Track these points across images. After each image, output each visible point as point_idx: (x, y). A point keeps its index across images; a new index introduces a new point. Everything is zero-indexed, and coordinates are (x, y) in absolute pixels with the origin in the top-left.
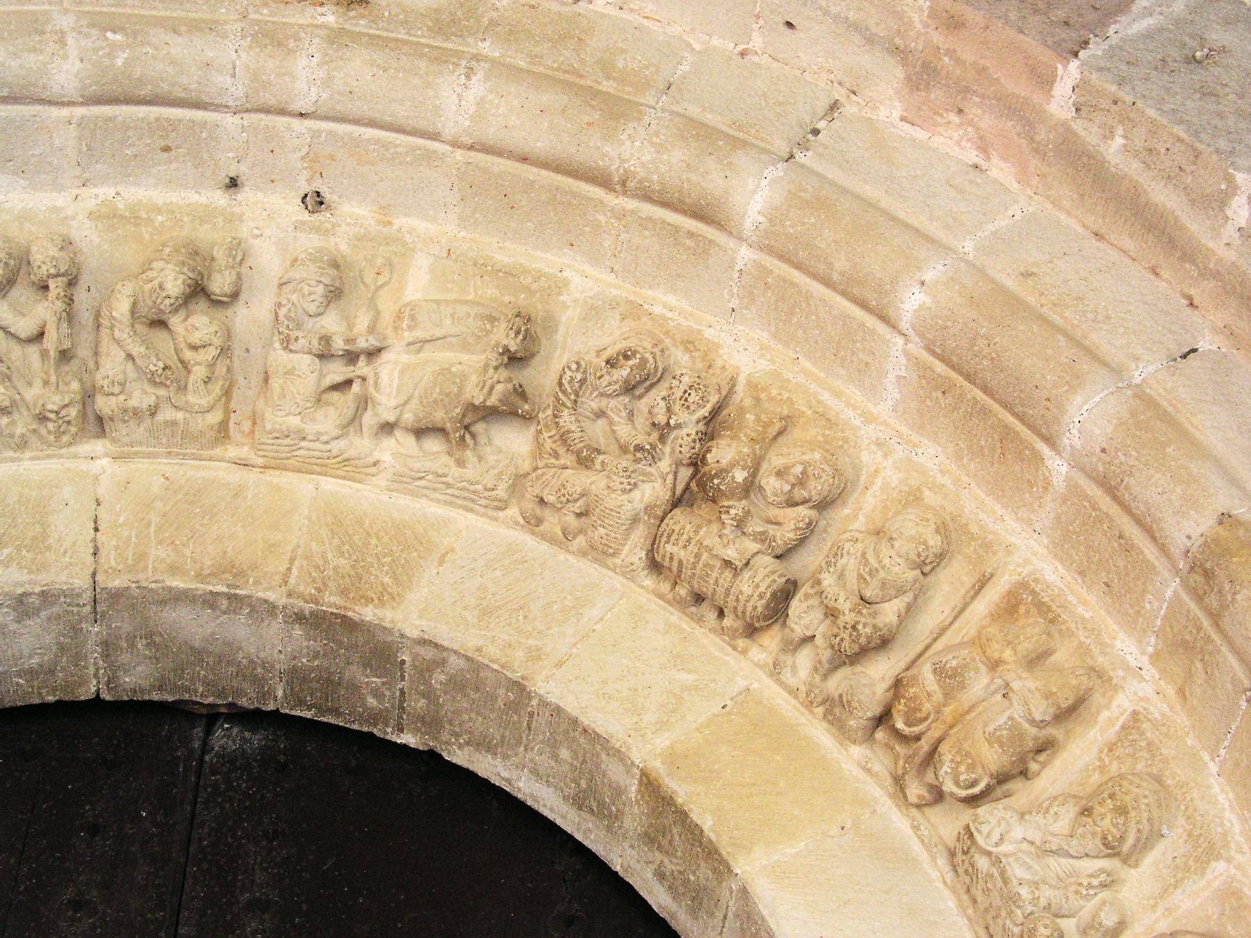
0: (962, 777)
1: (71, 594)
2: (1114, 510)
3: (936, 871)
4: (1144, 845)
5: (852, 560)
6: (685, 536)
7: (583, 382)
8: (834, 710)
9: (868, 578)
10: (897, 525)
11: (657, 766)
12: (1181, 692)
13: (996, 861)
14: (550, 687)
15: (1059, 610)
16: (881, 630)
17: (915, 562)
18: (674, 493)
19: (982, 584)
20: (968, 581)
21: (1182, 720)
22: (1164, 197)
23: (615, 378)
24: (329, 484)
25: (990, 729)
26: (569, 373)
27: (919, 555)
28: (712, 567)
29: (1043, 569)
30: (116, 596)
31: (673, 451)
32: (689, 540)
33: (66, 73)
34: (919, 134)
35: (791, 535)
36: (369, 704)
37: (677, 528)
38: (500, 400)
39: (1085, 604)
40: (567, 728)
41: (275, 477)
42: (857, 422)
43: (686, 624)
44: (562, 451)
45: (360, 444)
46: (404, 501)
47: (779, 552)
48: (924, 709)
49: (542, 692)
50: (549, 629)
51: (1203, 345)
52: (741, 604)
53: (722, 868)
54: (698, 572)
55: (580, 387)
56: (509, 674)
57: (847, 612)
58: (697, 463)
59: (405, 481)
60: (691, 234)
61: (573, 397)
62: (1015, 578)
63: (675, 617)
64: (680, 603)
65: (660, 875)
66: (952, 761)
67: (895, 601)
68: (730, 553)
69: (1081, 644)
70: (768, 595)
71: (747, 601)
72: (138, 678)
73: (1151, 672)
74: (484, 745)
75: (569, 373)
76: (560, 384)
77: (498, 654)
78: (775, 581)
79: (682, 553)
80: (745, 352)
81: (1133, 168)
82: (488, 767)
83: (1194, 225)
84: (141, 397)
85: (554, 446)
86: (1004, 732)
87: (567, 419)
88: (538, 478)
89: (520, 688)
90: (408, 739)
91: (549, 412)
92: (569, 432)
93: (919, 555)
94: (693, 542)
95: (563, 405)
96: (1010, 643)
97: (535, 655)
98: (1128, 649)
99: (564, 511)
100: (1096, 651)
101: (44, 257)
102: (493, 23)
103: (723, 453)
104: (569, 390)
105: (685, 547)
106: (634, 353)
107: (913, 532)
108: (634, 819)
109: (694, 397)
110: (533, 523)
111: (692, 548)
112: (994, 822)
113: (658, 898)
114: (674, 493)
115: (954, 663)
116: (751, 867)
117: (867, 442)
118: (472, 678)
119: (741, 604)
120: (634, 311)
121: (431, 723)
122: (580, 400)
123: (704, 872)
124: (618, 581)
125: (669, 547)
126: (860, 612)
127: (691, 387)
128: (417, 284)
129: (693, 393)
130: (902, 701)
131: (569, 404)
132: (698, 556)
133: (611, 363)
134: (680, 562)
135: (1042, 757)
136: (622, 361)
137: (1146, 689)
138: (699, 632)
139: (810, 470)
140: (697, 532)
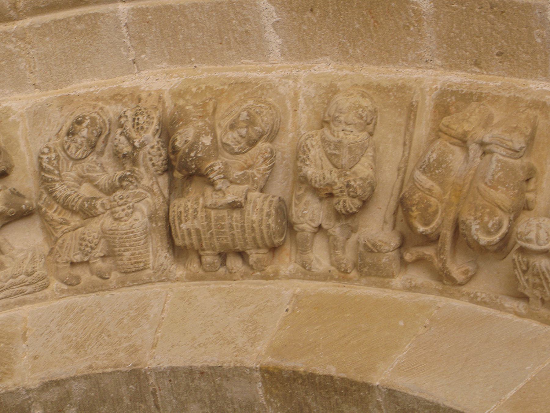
0: (490, 225)
5: (317, 150)
6: (191, 211)
7: (58, 158)
9: (337, 152)
10: (333, 109)
14: (159, 359)
15: (479, 91)
16: (367, 179)
17: (361, 124)
18: (163, 196)
20: (402, 120)
23: (79, 140)
25: (489, 177)
26: (45, 157)
27: (361, 117)
28: (222, 218)
29: (449, 79)
31: (147, 169)
32: (195, 210)
35: (264, 167)
37: (182, 209)
38: (6, 205)
42: (262, 75)
44: (68, 216)
47: (261, 183)
48: (432, 203)
49: (154, 366)
50: (131, 333)
52: (257, 231)
54: (214, 230)
55: (58, 162)
56: (122, 369)
57: (336, 180)
60: (79, 19)
61: (56, 172)
62: (434, 95)
66: (475, 219)
67: (363, 159)
68: (230, 198)
69: (509, 99)
70: (273, 212)
71: (260, 225)
75: (45, 157)
76: (42, 168)
77: (106, 363)
78: (271, 201)
79: (196, 223)
85: (61, 216)
86: (500, 174)
87: (60, 190)
88: (61, 247)
89: (137, 375)
91: (45, 196)
92: (67, 196)
93: (361, 117)
94: (199, 210)
95: (53, 181)
96: (463, 120)
99: (91, 262)
100: (522, 95)
104: (52, 168)
105: (195, 217)
106: (84, 117)
107: (348, 104)
109: (142, 119)
111: (201, 214)
112: (534, 228)
114: (164, 198)
115: (434, 156)
117: (277, 80)
119: (257, 231)
122: (62, 174)
125: (184, 226)
126: (345, 175)
127: (136, 115)
129: (141, 117)
130: (414, 208)
131: (56, 178)
132: (208, 217)
133: (71, 133)
134: (197, 231)
135: (532, 186)
136: (78, 127)
139: (252, 111)
140: (197, 203)
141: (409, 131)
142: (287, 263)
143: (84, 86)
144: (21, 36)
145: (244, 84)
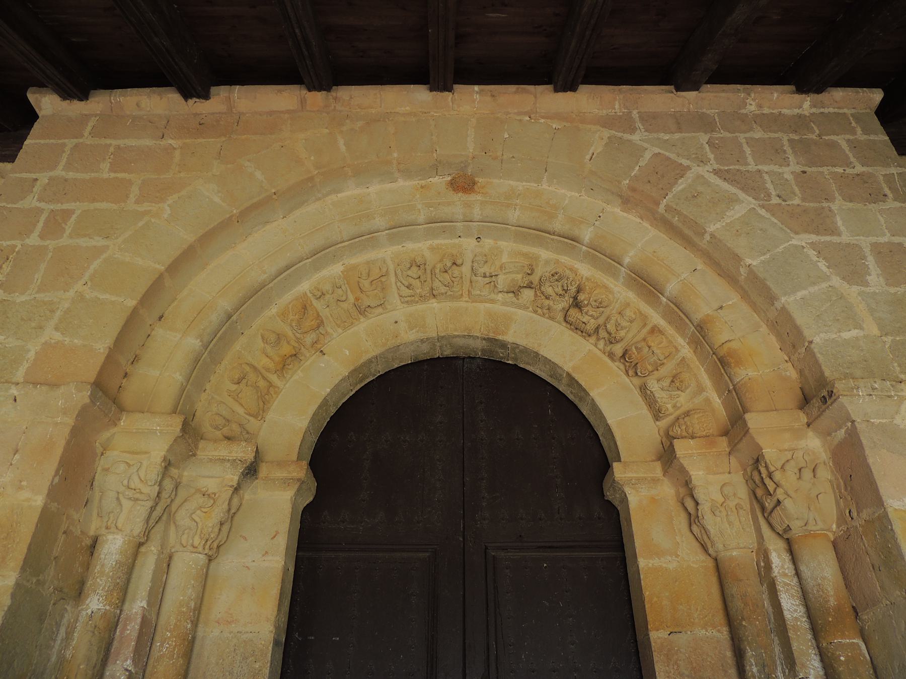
1: (433, 338)
2: (678, 310)
3: (636, 393)
4: (687, 388)
8: (611, 355)
11: (570, 371)
12: (694, 352)
13: (652, 392)
14: (545, 352)
19: (645, 325)
21: (695, 358)
22: (687, 231)
24: (487, 305)
30: (443, 337)
33: (421, 218)
34: (625, 214)
36: (500, 355)
39: (670, 330)
40: (547, 361)
41: (474, 304)
43: (573, 334)
45: (493, 296)
46: (505, 308)
51: (698, 268)
53: (587, 394)
58: (575, 298)
59: (504, 304)
63: (571, 332)
64: (571, 329)
65: (571, 393)
68: (584, 320)
72: (448, 352)
73: (687, 346)
74: (528, 364)
80: (585, 270)
81: (680, 225)
82: (528, 368)
83: (696, 239)
84: (443, 289)
87: (543, 288)
90: (510, 362)
97: (540, 345)
98: (681, 341)
101: (419, 260)
102: (519, 195)
103: (581, 297)
108: (565, 381)
110: (535, 312)
113: (571, 397)
116: (593, 394)
118: (525, 351)
120: (557, 262)
121: (516, 359)
123: (583, 394)
124: (556, 324)
128: (505, 259)
137: (686, 351)
138: (577, 336)
141: (641, 329)
142: (593, 339)
143: (564, 259)
144: (552, 240)
145: (606, 287)
